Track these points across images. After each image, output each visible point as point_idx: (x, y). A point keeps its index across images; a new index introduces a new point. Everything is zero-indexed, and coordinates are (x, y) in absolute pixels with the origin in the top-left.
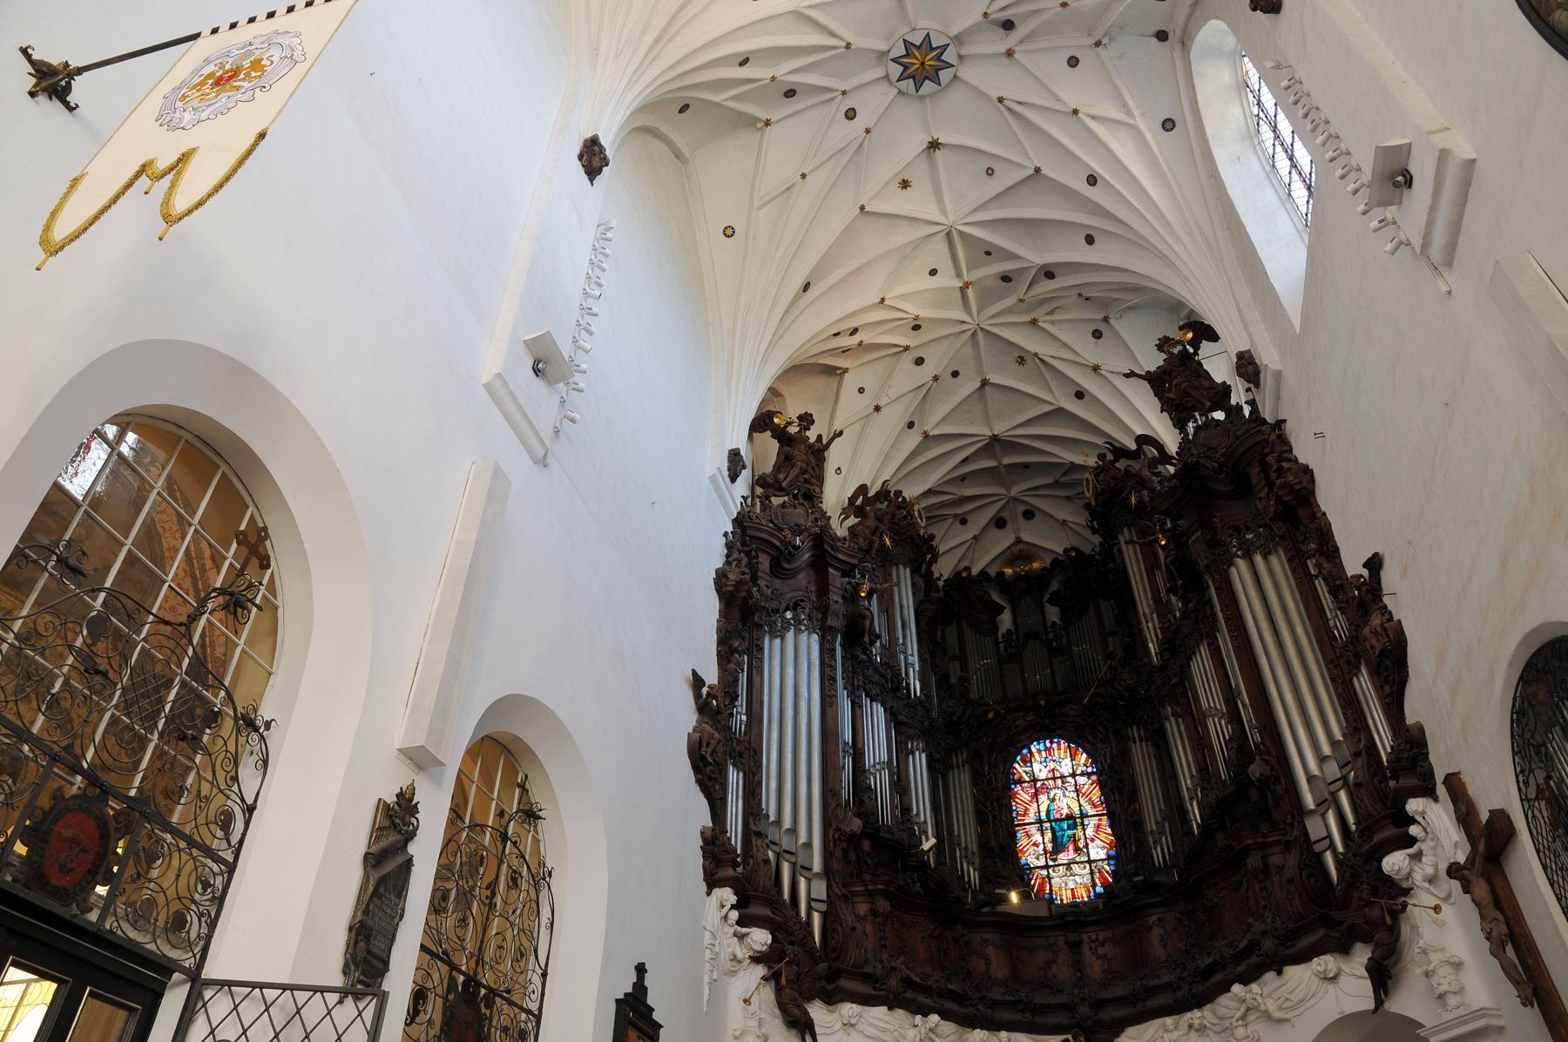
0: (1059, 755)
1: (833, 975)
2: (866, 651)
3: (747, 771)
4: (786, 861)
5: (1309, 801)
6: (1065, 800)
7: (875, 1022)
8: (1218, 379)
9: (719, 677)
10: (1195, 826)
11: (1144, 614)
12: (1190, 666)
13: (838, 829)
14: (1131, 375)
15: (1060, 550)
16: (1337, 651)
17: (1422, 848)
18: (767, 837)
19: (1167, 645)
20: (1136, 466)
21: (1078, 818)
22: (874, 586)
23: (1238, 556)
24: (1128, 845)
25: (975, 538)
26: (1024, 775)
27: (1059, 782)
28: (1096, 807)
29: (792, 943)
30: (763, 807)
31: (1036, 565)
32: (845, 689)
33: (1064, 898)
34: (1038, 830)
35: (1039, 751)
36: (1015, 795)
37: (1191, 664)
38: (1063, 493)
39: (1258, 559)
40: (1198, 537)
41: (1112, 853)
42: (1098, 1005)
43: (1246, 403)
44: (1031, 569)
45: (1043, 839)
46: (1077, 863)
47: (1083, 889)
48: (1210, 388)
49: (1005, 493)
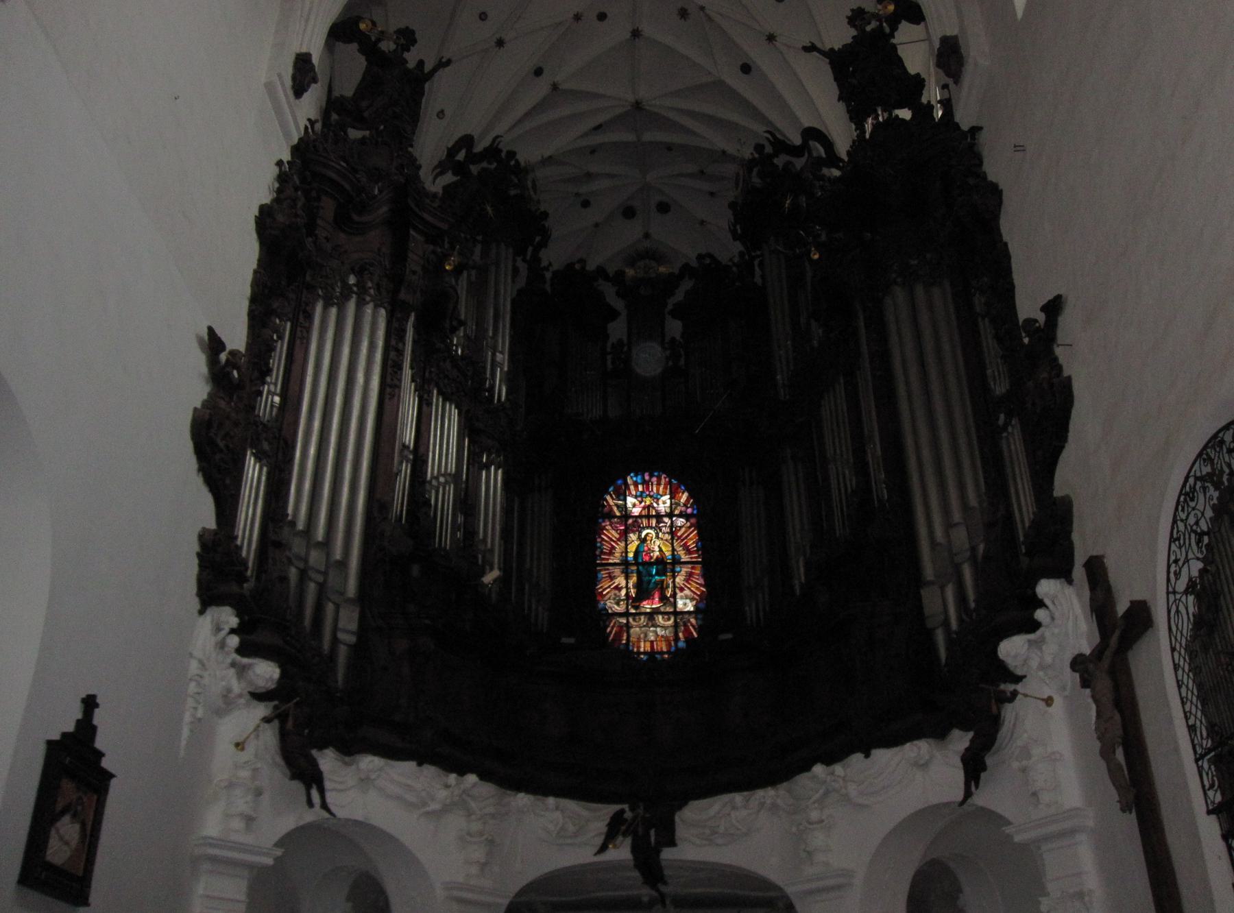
0: (658, 490)
5: (929, 572)
6: (658, 543)
8: (912, 70)
14: (810, 48)
18: (290, 549)
20: (799, 163)
25: (597, 225)
26: (615, 509)
27: (654, 522)
30: (290, 510)
31: (662, 269)
32: (413, 380)
34: (622, 572)
35: (636, 485)
39: (919, 290)
41: (702, 606)
43: (939, 102)
45: (627, 583)
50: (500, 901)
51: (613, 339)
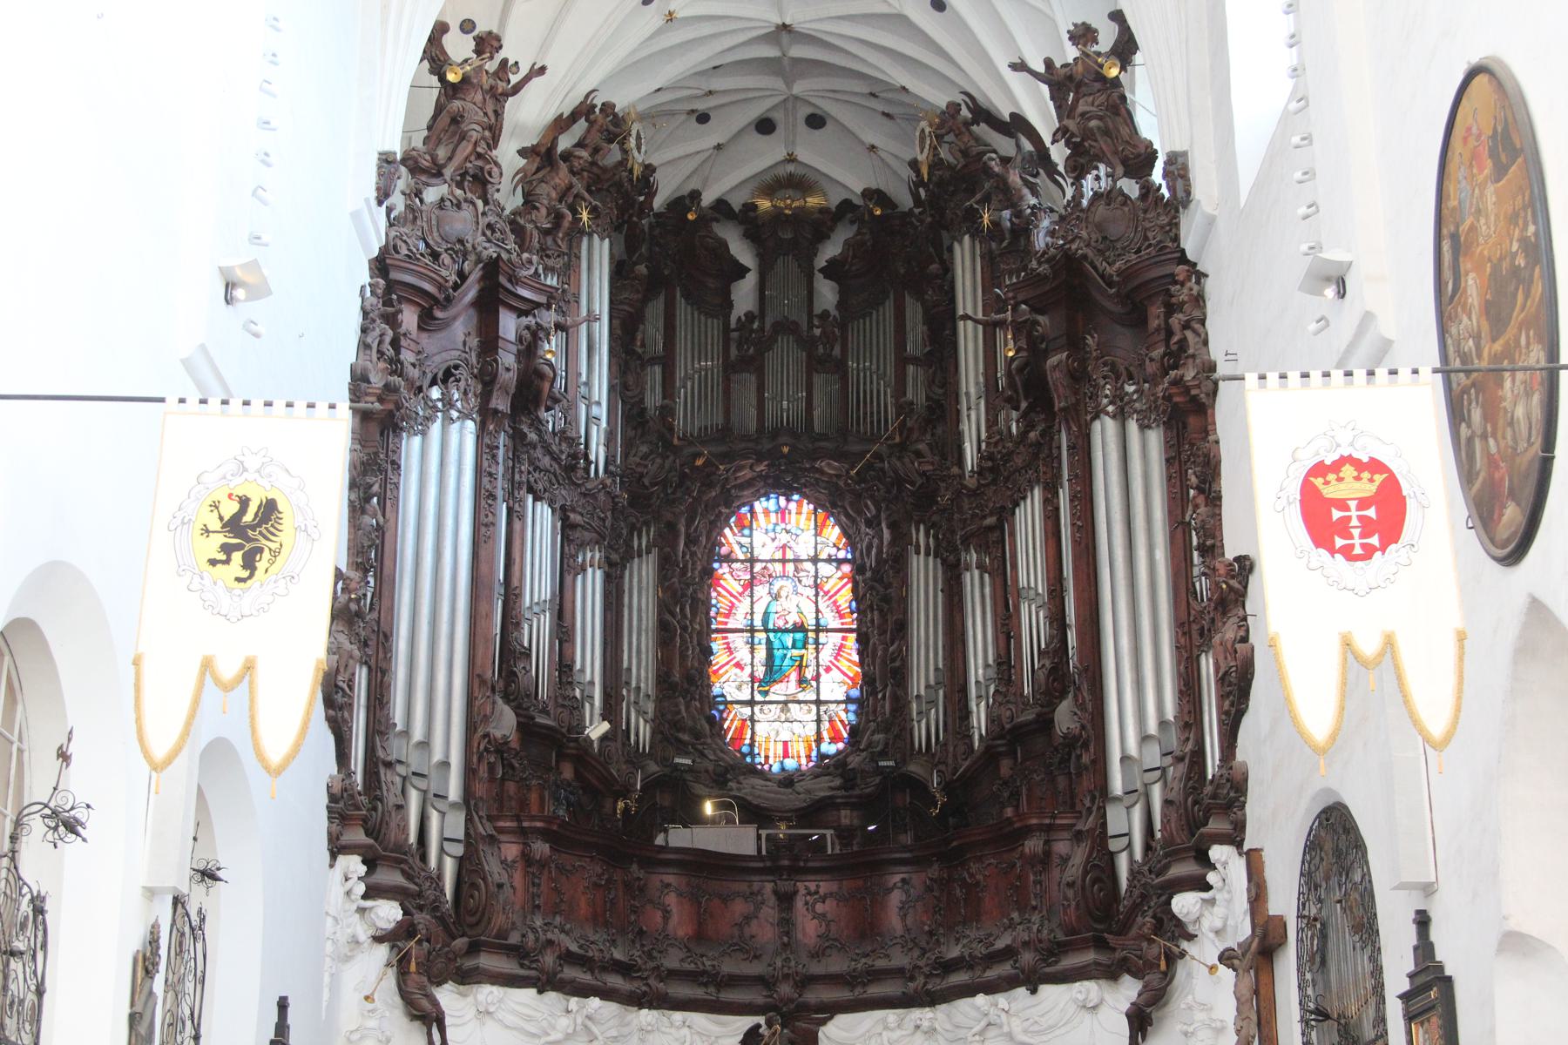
0: (798, 523)
2: (538, 424)
3: (374, 667)
4: (415, 787)
5: (1117, 785)
6: (795, 599)
7: (518, 1008)
9: (349, 540)
10: (976, 737)
11: (967, 394)
12: (1013, 513)
13: (486, 735)
14: (1020, 66)
16: (1193, 612)
17: (1217, 897)
19: (992, 463)
21: (812, 631)
22: (561, 319)
23: (1107, 414)
24: (880, 696)
25: (719, 147)
27: (790, 567)
28: (841, 616)
29: (421, 908)
31: (813, 201)
33: (771, 754)
34: (747, 643)
35: (767, 512)
36: (718, 580)
37: (1017, 511)
38: (881, 107)
40: (1061, 361)
41: (855, 693)
42: (807, 981)
44: (802, 209)
46: (799, 702)
47: (802, 744)
48: (1128, 142)
49: (787, 91)
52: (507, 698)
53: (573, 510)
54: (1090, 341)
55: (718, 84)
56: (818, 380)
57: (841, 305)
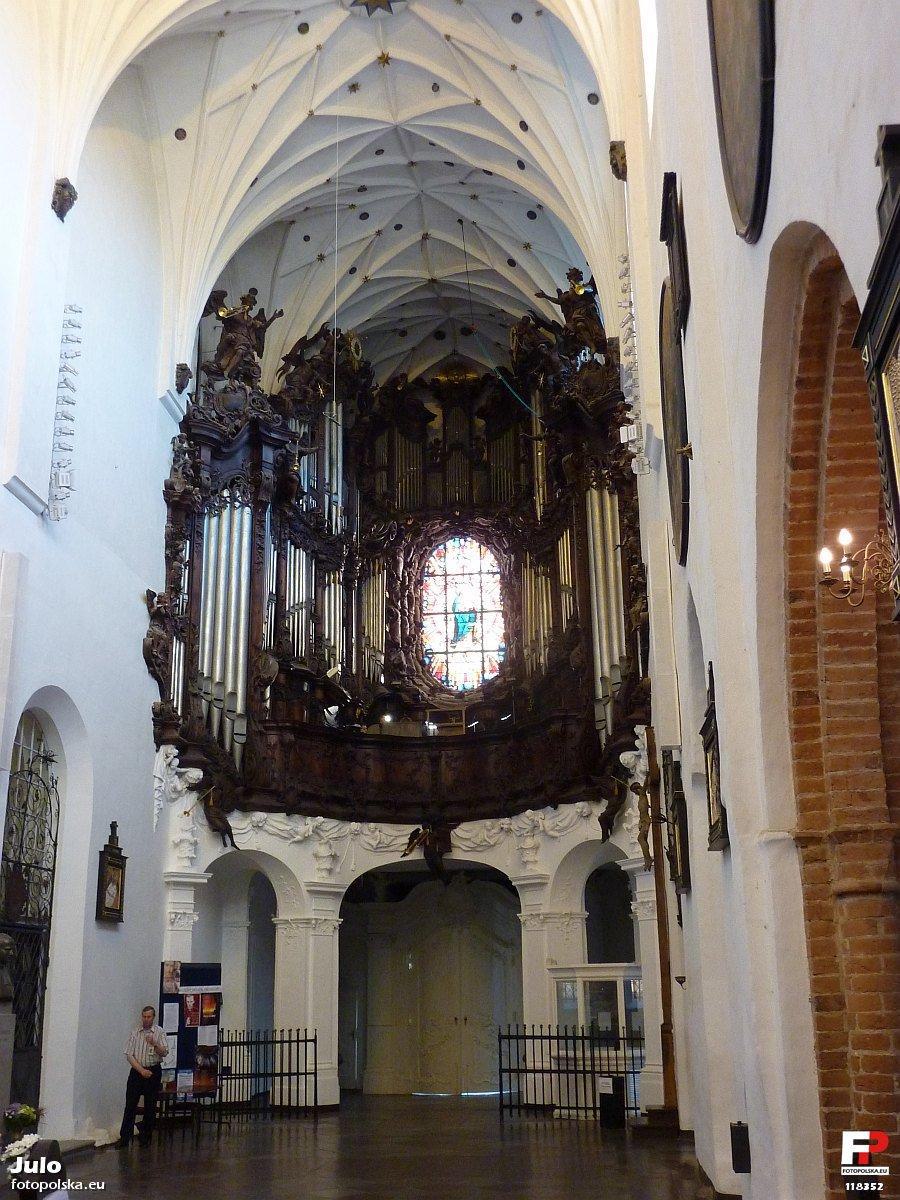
1: (248, 793)
2: (295, 509)
5: (600, 693)
11: (538, 479)
15: (492, 365)
23: (592, 486)
25: (413, 349)
29: (218, 772)
31: (471, 376)
41: (503, 645)
50: (341, 890)
51: (431, 439)
52: (276, 655)
53: (322, 553)
54: (584, 446)
55: (408, 314)
56: (475, 474)
57: (487, 432)
